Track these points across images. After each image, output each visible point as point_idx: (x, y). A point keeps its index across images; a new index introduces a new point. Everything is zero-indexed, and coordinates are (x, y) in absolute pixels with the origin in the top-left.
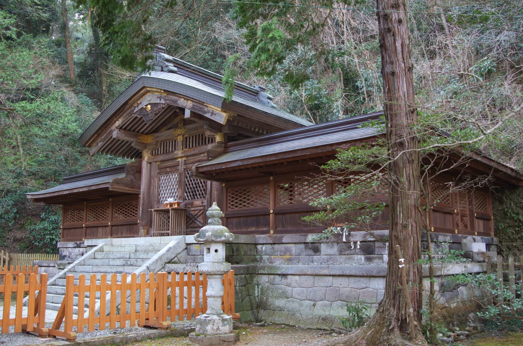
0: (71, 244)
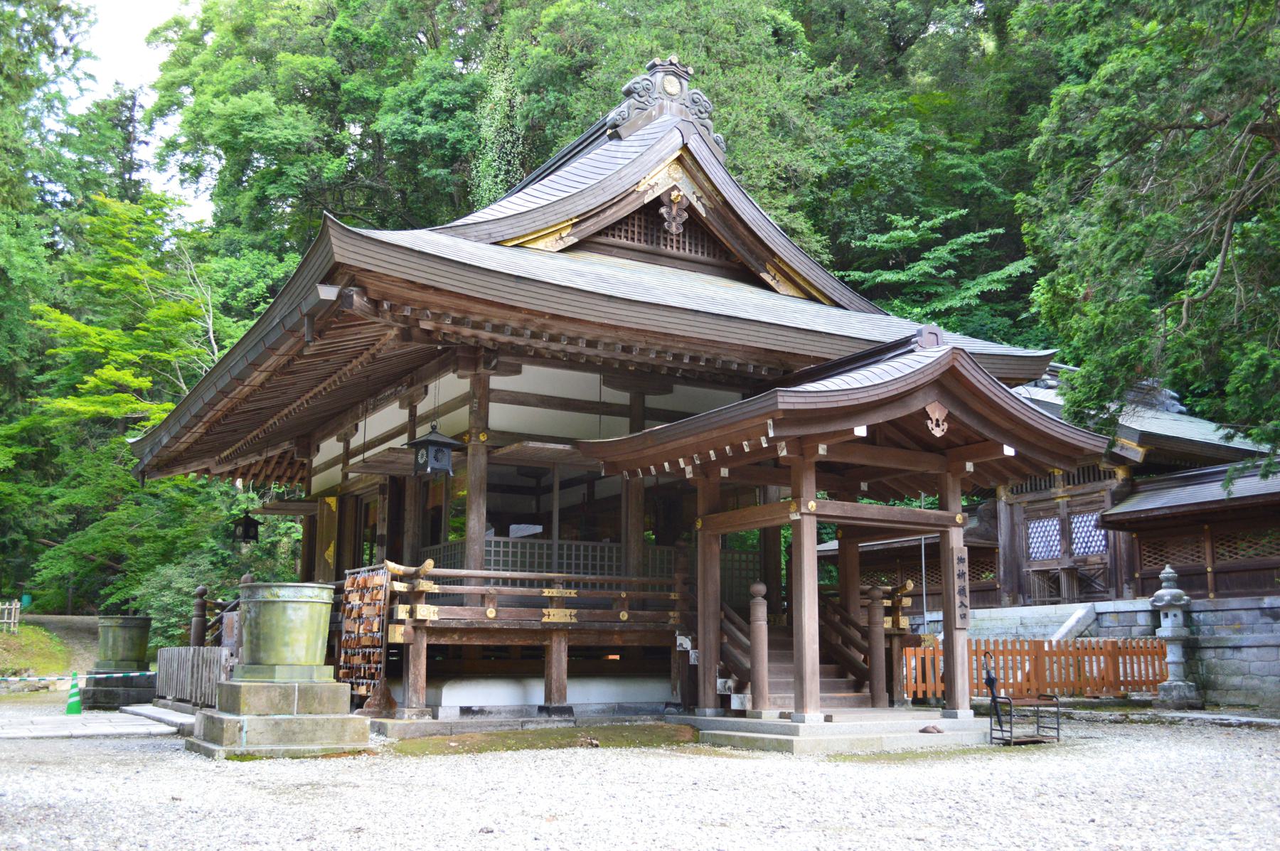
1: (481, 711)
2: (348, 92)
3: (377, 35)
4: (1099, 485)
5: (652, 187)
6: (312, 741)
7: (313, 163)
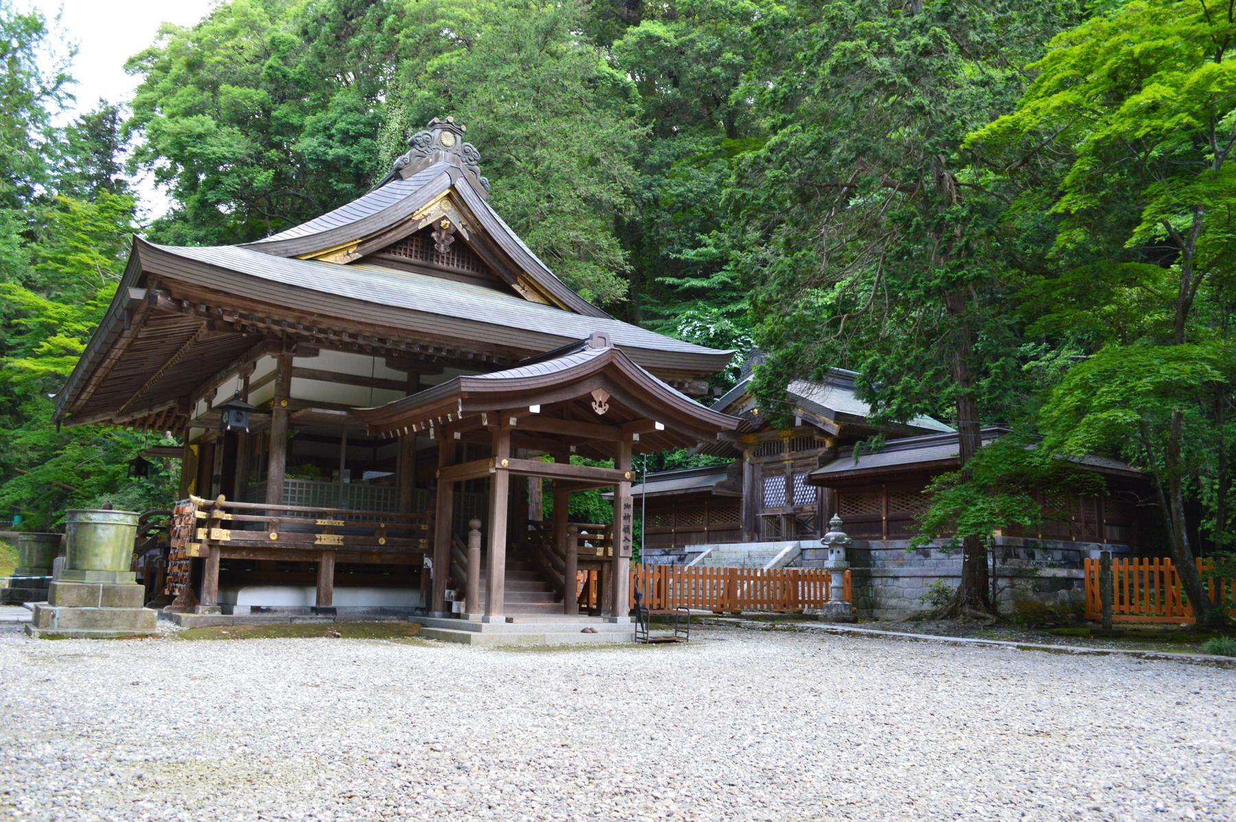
0: (657, 552)
1: (268, 610)
2: (277, 118)
3: (302, 73)
4: (813, 452)
5: (425, 217)
6: (110, 627)
7: (246, 174)
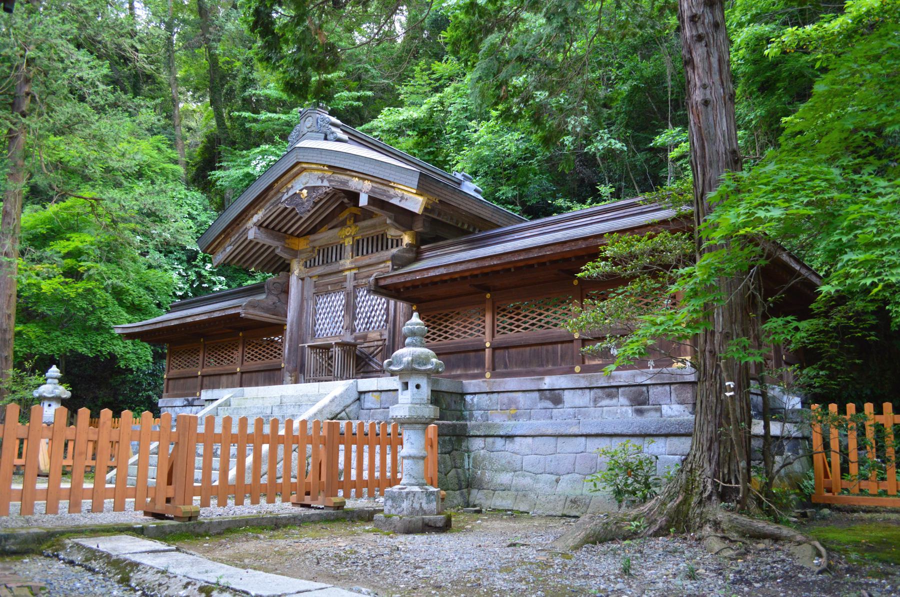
0: (179, 402)
